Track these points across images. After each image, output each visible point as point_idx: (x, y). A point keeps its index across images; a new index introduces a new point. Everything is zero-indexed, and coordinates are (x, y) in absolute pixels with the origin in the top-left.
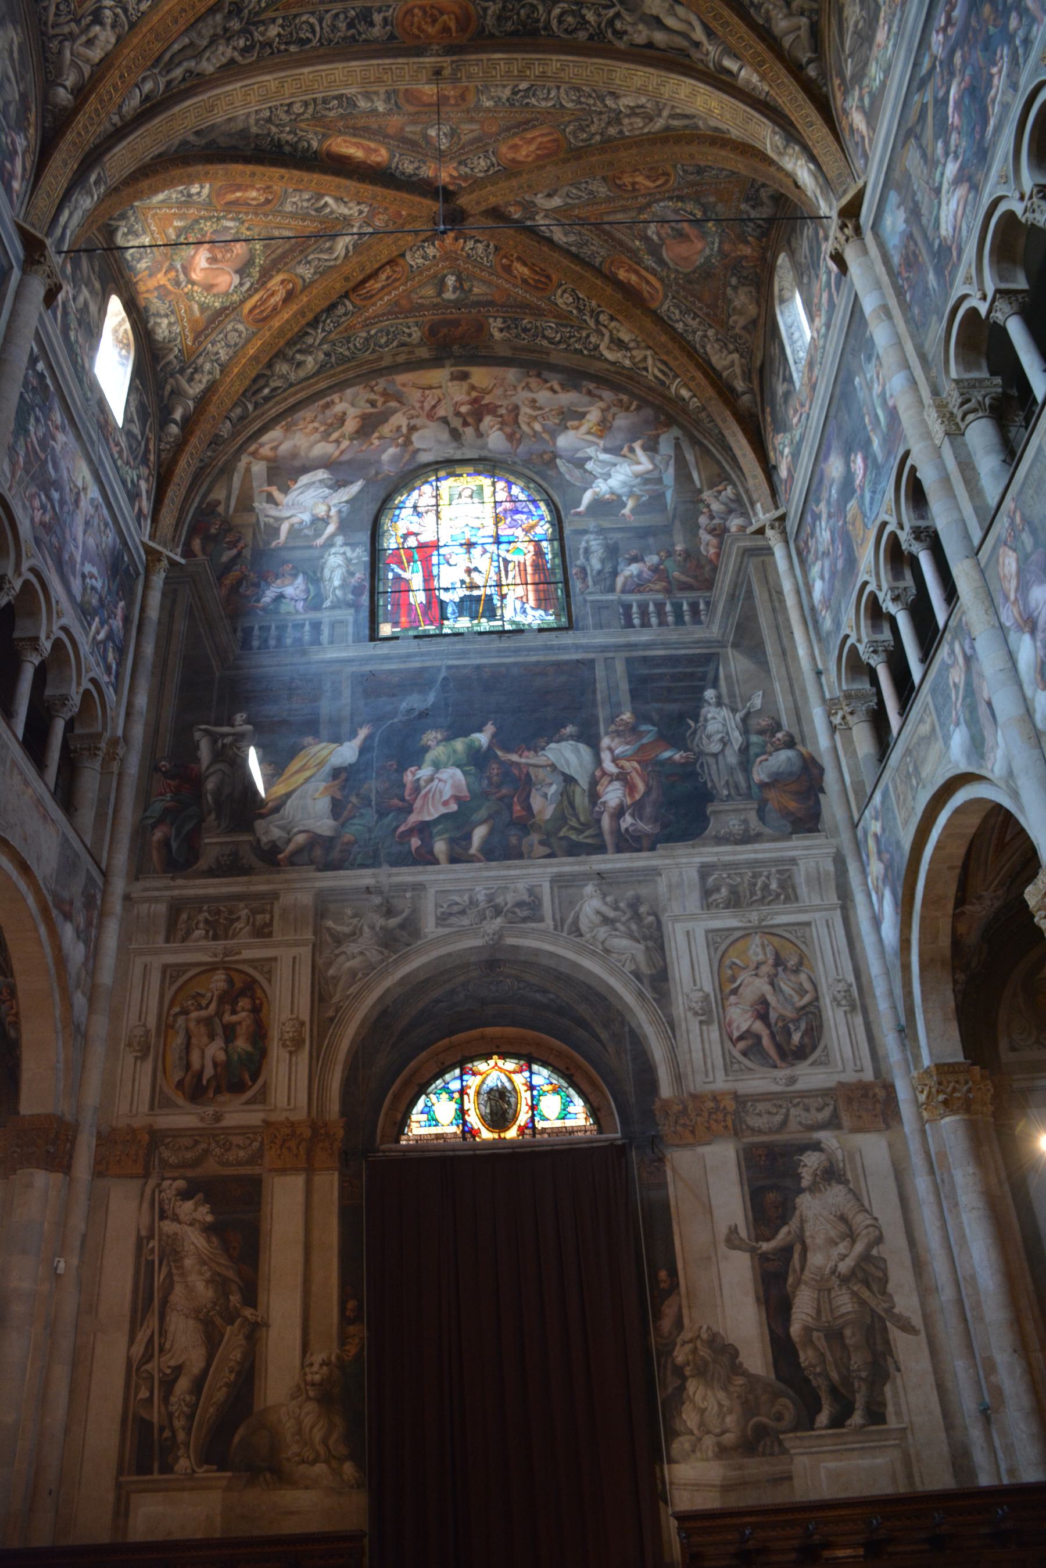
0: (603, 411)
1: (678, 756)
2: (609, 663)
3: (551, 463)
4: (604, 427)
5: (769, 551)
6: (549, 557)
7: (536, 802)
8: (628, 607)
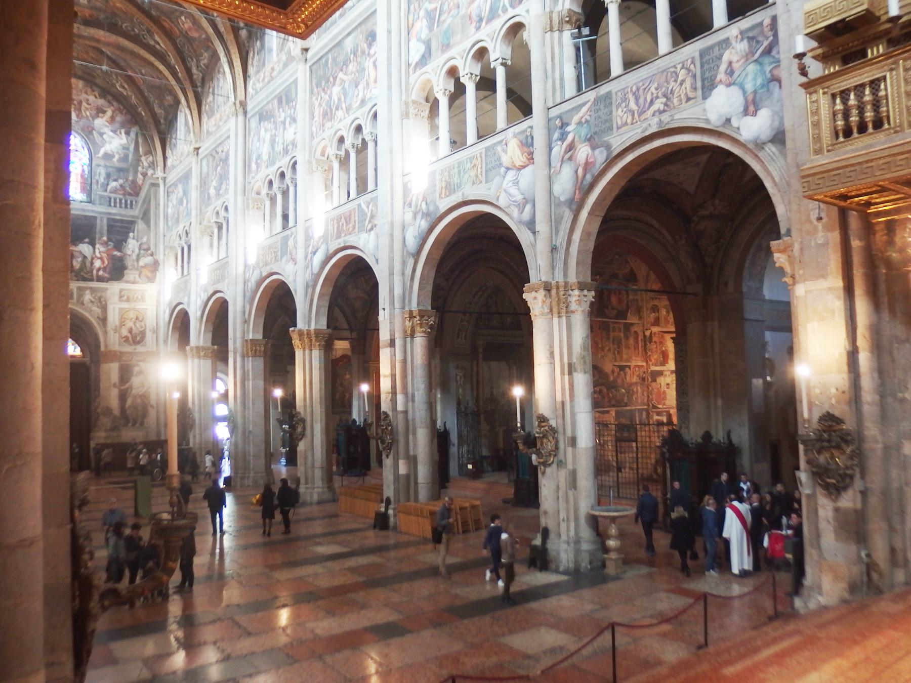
0: (113, 112)
1: (119, 254)
2: (102, 218)
3: (91, 132)
4: (112, 119)
5: (157, 185)
6: (86, 172)
7: (75, 263)
8: (110, 199)
